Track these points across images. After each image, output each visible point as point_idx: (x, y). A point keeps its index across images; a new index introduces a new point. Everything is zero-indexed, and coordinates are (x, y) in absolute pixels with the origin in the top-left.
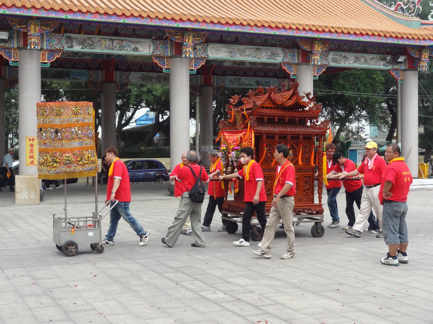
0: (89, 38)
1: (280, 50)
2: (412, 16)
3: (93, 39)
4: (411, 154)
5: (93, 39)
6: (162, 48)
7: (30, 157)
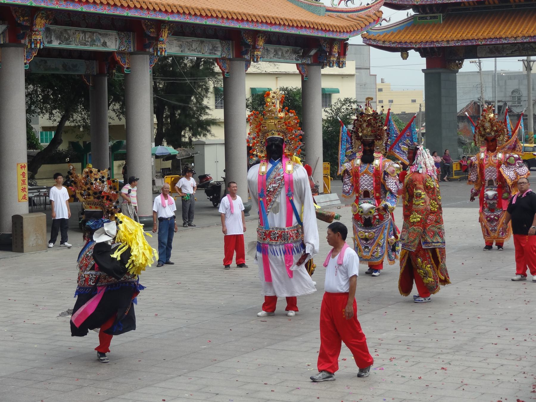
0: (66, 30)
1: (218, 42)
3: (69, 31)
4: (318, 165)
5: (69, 31)
6: (126, 41)
7: (22, 190)
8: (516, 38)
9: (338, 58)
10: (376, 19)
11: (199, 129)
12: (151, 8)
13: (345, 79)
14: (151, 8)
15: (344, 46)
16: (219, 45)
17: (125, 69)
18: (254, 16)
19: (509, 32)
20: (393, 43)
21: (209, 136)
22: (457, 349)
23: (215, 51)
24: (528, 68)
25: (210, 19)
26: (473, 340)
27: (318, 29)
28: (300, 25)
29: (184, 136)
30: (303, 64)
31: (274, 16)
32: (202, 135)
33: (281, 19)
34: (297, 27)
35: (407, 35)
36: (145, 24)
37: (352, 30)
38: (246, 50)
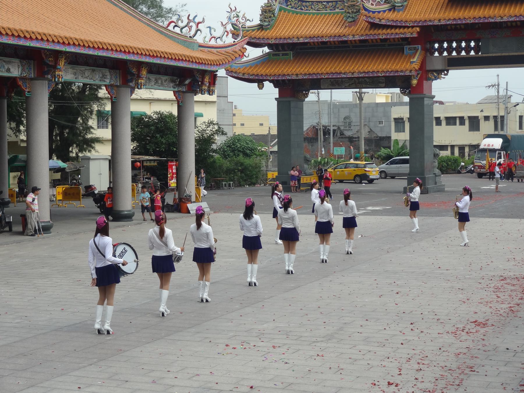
2: (190, 37)
6: (27, 68)
8: (353, 73)
9: (209, 87)
10: (241, 54)
11: (85, 146)
12: (51, 40)
13: (208, 105)
14: (51, 40)
15: (214, 77)
16: (108, 74)
17: (26, 93)
18: (139, 49)
19: (347, 68)
20: (251, 75)
21: (93, 152)
22: (329, 338)
23: (105, 78)
24: (361, 99)
25: (101, 51)
26: (341, 329)
27: (192, 62)
28: (177, 58)
29: (72, 152)
30: (179, 91)
31: (155, 49)
32: (87, 151)
33: (162, 52)
34: (175, 59)
35: (263, 69)
36: (45, 54)
37: (221, 63)
38: (132, 78)
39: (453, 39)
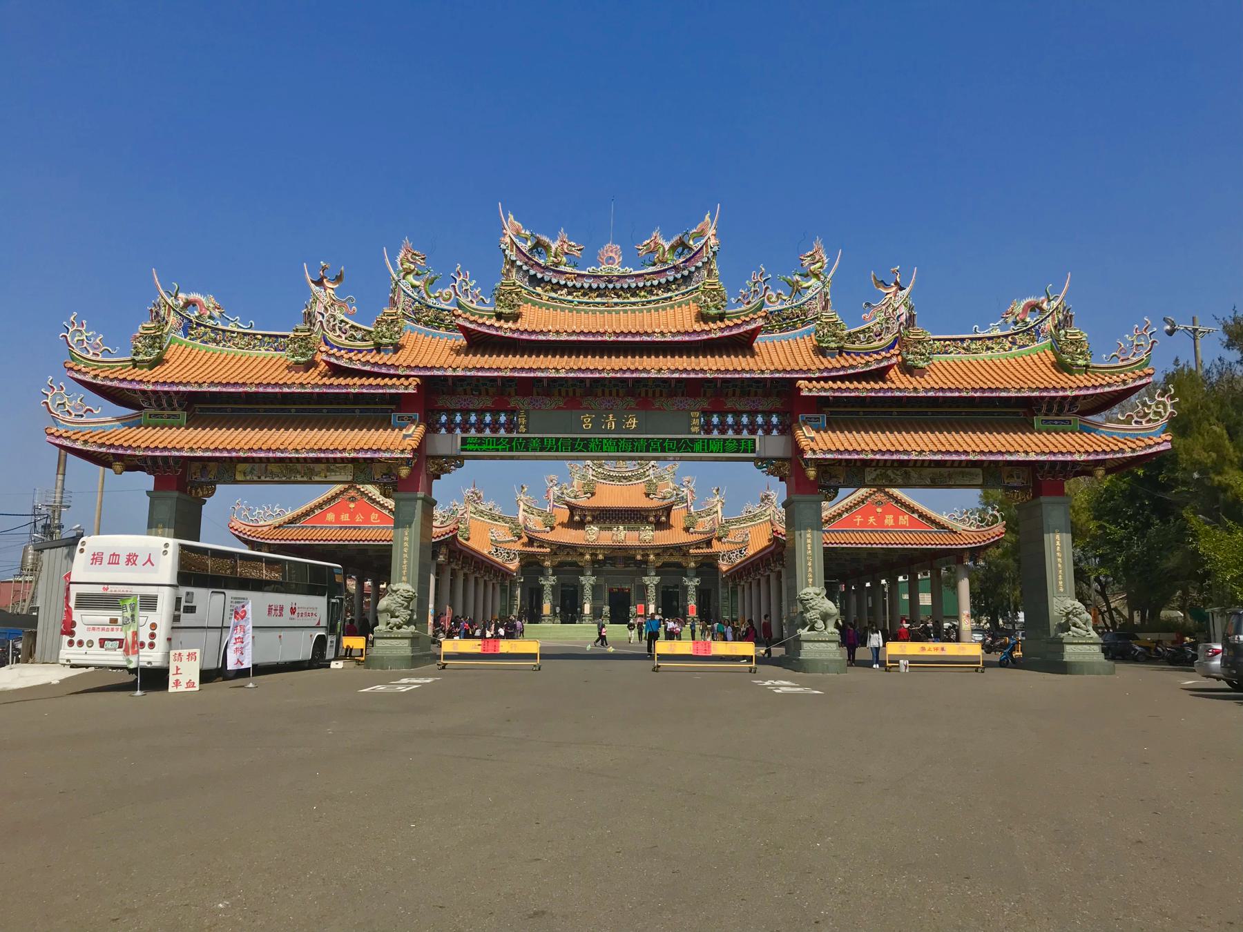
39: (471, 407)
